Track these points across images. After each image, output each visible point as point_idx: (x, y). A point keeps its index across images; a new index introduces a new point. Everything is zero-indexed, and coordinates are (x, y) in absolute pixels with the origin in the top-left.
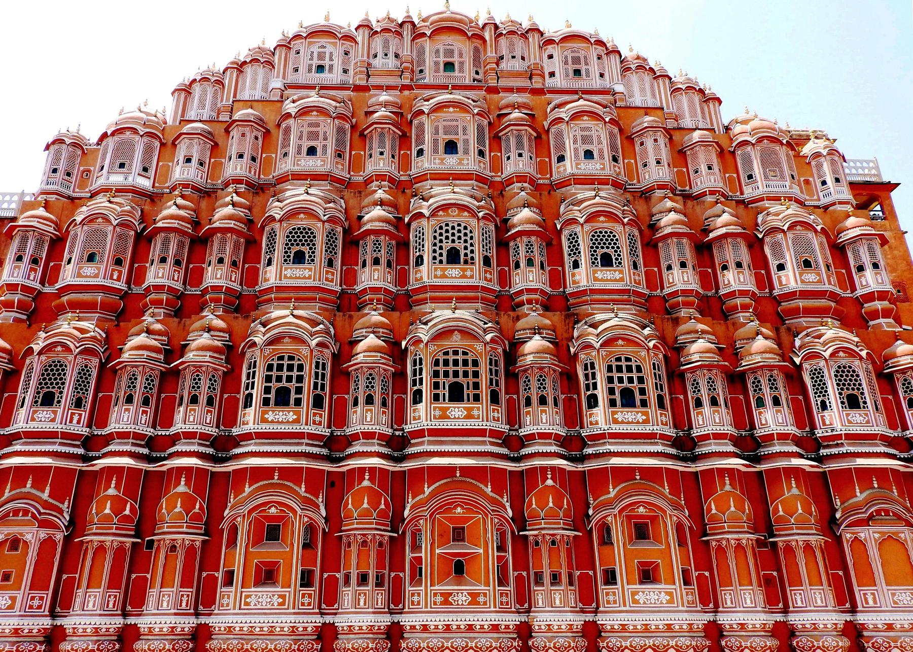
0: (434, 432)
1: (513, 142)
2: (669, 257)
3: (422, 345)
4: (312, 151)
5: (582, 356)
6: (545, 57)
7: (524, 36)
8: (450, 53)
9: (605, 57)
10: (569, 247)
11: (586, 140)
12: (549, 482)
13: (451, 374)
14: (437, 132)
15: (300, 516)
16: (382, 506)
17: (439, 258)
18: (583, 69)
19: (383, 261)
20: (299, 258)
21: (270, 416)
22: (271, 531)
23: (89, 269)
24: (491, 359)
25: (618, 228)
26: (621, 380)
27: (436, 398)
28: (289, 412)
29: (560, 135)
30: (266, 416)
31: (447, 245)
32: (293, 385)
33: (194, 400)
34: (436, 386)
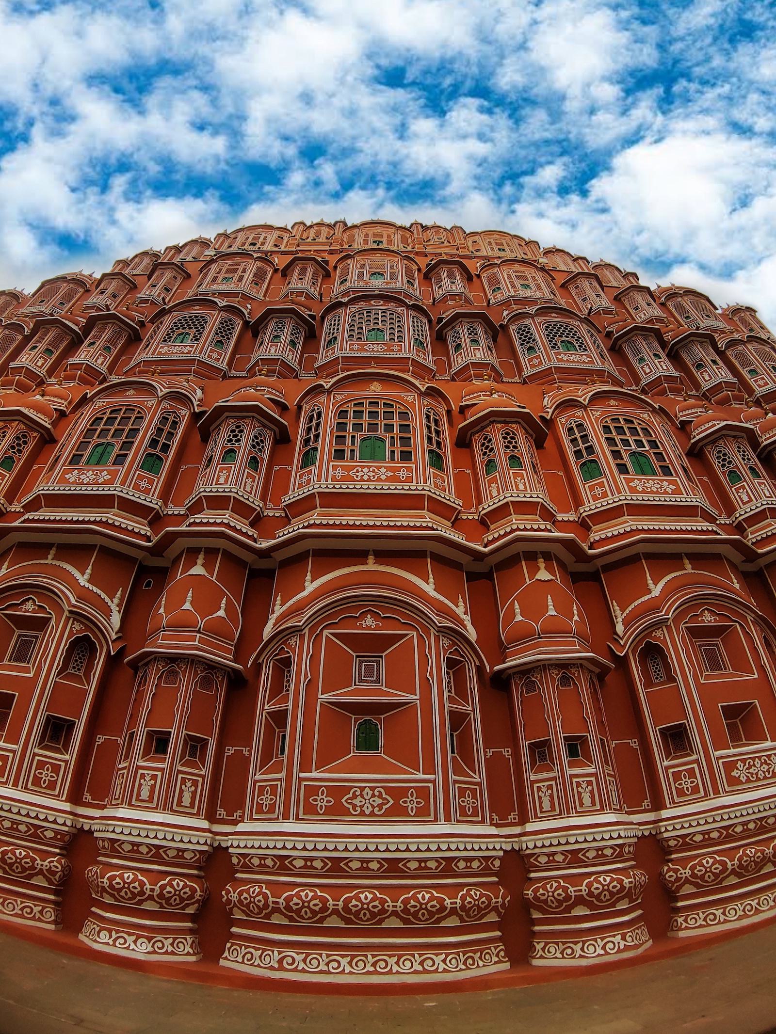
0: (332, 500)
1: (444, 275)
2: (637, 351)
3: (323, 398)
7: (450, 231)
10: (520, 338)
12: (543, 575)
13: (365, 427)
14: (362, 267)
15: (68, 619)
16: (221, 613)
17: (356, 337)
21: (72, 477)
24: (428, 417)
25: (576, 323)
26: (626, 442)
27: (339, 454)
28: (102, 471)
30: (67, 476)
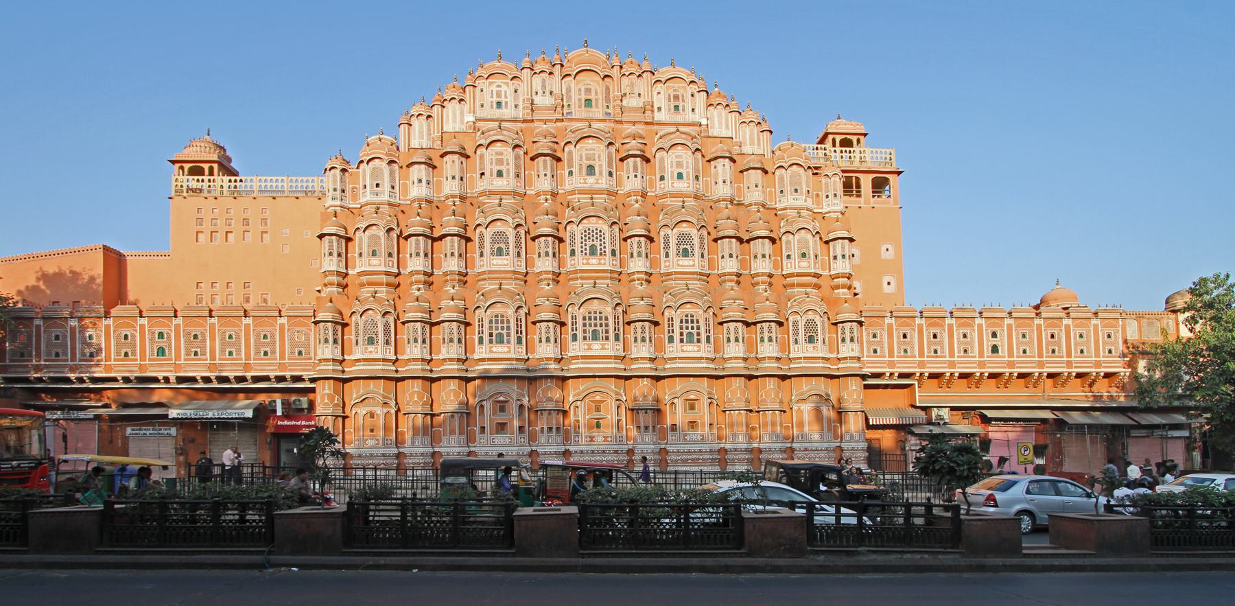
0: (584, 357)
4: (500, 174)
5: (666, 313)
6: (655, 94)
8: (588, 91)
9: (696, 94)
11: (679, 164)
18: (681, 104)
19: (551, 254)
20: (500, 252)
21: (494, 349)
22: (502, 407)
23: (375, 261)
27: (585, 338)
29: (662, 160)
31: (589, 243)
32: (504, 332)
33: (451, 341)
34: (585, 332)
